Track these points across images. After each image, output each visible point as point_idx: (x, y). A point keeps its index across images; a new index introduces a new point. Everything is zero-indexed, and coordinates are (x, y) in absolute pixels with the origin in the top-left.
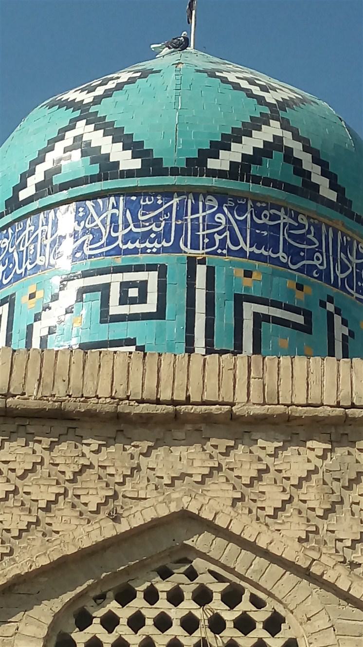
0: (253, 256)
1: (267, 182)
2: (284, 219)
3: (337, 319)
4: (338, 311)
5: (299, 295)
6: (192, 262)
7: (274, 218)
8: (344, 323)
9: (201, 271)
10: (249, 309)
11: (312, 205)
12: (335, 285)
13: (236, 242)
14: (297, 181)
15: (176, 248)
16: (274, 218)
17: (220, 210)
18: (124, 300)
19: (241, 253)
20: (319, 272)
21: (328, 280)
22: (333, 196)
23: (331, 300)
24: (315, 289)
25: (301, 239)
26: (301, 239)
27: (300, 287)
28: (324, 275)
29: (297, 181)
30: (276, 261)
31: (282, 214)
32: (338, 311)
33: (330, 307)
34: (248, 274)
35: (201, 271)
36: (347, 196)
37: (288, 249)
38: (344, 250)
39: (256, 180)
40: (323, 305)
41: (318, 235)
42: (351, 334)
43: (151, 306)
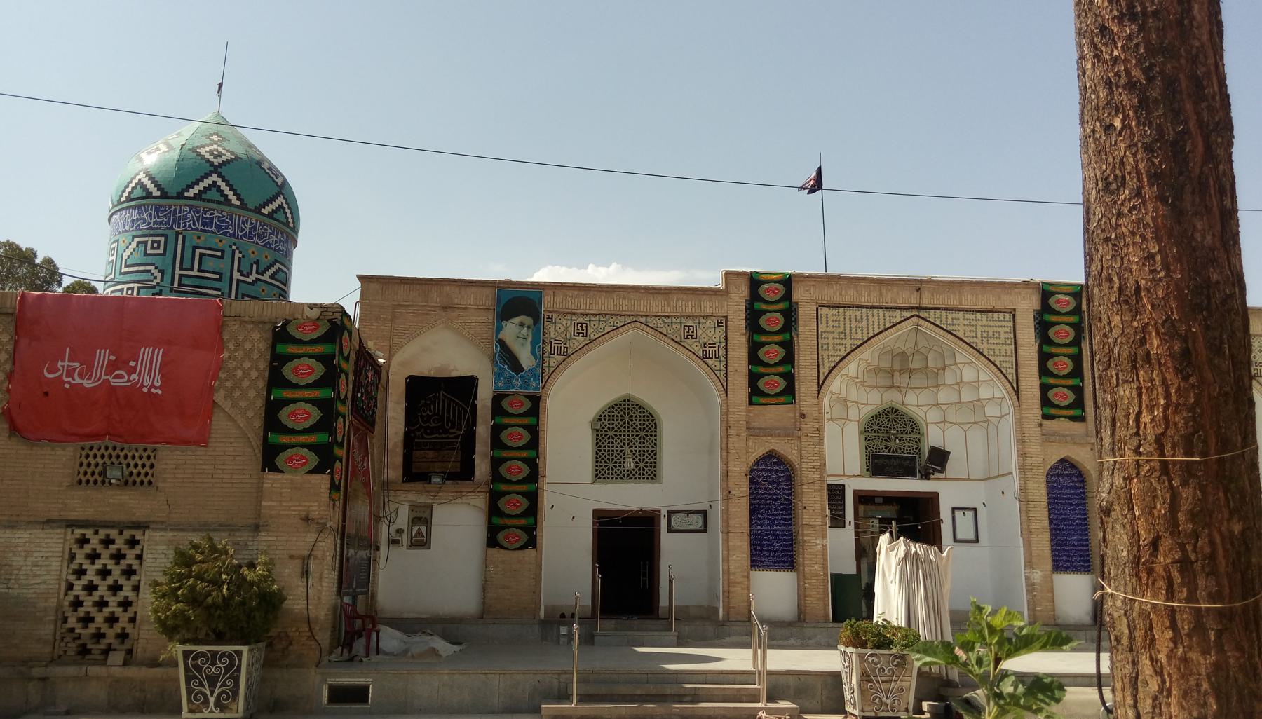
0: (202, 230)
1: (209, 201)
2: (216, 214)
3: (237, 252)
4: (237, 248)
5: (220, 244)
6: (177, 234)
7: (211, 214)
8: (240, 252)
9: (180, 237)
10: (198, 251)
11: (228, 208)
12: (238, 238)
13: (195, 225)
14: (222, 199)
15: (171, 228)
16: (211, 214)
17: (190, 212)
18: (152, 248)
19: (197, 229)
20: (230, 234)
21: (234, 237)
22: (238, 203)
23: (234, 244)
24: (228, 240)
25: (224, 221)
26: (224, 221)
27: (220, 241)
28: (233, 235)
29: (222, 199)
30: (212, 232)
31: (215, 212)
32: (237, 248)
33: (234, 247)
34: (199, 238)
35: (180, 237)
36: (245, 201)
37: (217, 226)
38: (243, 223)
39: (204, 200)
40: (231, 247)
41: (231, 220)
42: (243, 256)
43: (161, 251)
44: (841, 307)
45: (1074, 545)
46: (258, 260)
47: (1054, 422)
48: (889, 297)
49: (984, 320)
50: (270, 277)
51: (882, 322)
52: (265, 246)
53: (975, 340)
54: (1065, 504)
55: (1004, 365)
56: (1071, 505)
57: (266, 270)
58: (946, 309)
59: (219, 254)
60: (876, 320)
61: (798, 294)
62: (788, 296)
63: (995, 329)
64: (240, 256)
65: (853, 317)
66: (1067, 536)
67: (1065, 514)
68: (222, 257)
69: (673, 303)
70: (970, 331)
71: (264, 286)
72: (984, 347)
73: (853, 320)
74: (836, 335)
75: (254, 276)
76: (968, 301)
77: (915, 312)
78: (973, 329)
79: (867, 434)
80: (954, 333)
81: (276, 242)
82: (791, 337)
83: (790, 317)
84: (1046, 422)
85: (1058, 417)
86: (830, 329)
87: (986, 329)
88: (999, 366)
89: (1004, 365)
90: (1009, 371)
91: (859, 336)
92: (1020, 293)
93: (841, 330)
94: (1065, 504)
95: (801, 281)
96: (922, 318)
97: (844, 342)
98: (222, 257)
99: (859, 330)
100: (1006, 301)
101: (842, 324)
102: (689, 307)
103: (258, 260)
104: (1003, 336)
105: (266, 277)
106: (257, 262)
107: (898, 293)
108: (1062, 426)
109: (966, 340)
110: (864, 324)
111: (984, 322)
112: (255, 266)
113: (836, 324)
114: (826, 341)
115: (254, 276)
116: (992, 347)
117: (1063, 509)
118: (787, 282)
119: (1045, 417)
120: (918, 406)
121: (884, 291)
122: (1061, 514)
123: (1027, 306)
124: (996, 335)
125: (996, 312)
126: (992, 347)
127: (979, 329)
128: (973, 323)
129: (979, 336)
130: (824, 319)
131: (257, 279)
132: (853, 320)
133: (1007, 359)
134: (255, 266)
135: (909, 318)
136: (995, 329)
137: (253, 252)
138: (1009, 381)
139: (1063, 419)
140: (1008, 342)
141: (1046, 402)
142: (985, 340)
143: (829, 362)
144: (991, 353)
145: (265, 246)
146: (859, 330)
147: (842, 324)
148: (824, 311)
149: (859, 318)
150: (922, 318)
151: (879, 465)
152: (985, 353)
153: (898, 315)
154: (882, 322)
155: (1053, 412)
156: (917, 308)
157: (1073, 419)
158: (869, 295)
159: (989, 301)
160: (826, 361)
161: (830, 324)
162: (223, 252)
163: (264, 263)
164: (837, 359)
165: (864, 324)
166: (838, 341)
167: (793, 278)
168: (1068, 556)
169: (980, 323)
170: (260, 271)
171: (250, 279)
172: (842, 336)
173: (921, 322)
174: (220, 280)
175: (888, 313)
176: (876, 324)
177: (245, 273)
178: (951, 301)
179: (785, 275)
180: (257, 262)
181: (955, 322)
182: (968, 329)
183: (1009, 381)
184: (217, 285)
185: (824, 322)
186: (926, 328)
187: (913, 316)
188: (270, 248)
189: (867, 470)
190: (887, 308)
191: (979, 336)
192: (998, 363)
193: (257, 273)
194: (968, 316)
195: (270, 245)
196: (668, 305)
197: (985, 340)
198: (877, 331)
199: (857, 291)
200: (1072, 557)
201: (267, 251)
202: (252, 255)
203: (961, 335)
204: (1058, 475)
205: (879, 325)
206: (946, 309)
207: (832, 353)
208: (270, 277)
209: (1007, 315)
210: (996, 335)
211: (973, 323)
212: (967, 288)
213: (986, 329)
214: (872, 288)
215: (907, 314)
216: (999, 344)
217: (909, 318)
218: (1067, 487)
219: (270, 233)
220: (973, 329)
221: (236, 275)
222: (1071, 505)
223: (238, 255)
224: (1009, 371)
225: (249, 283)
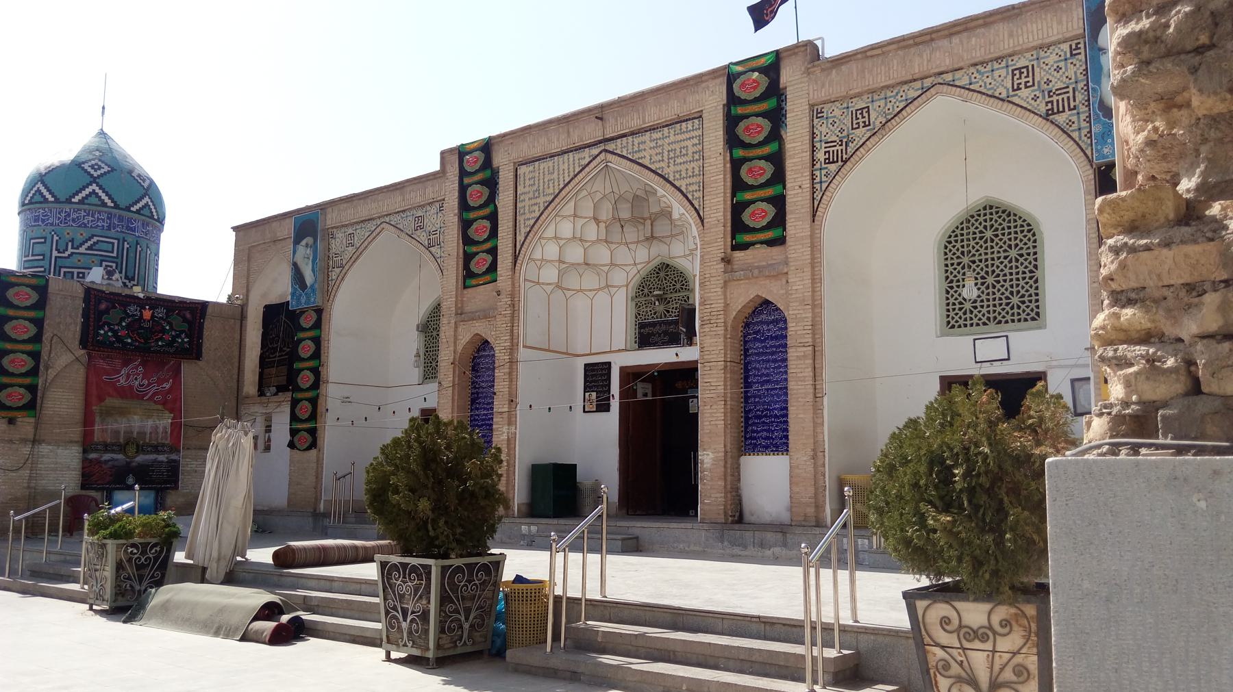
42: (60, 238)
44: (537, 161)
45: (776, 416)
46: (73, 239)
47: (748, 252)
48: (576, 138)
49: (670, 135)
50: (86, 249)
51: (571, 169)
52: (79, 226)
53: (662, 164)
54: (768, 361)
55: (690, 189)
56: (775, 361)
57: (81, 245)
58: (633, 134)
59: (43, 240)
60: (567, 165)
61: (501, 160)
62: (487, 163)
63: (683, 144)
64: (58, 238)
65: (546, 170)
66: (769, 404)
67: (767, 375)
68: (45, 242)
69: (407, 196)
70: (656, 155)
71: (79, 257)
72: (669, 172)
73: (546, 173)
74: (531, 195)
75: (70, 250)
76: (653, 115)
77: (602, 147)
78: (660, 150)
79: (637, 300)
80: (640, 161)
81: (92, 221)
82: (496, 207)
83: (492, 184)
84: (738, 255)
85: (753, 244)
86: (527, 189)
87: (673, 146)
88: (685, 191)
89: (690, 189)
90: (696, 195)
91: (551, 191)
92: (708, 87)
93: (535, 188)
94: (768, 361)
95: (501, 141)
96: (610, 152)
97: (538, 200)
98: (45, 242)
99: (551, 185)
100: (691, 104)
101: (536, 182)
102: (415, 197)
103: (73, 239)
104: (690, 152)
105: (82, 250)
106: (72, 241)
107: (584, 129)
108: (758, 255)
109: (653, 167)
110: (555, 175)
111: (672, 139)
112: (70, 244)
113: (532, 182)
114: (522, 204)
115: (70, 250)
116: (678, 168)
117: (766, 368)
118: (487, 147)
119: (734, 248)
120: (685, 256)
121: (571, 130)
122: (763, 375)
123: (713, 102)
124: (684, 152)
125: (684, 121)
126: (678, 168)
127: (667, 148)
128: (660, 142)
129: (666, 158)
130: (522, 179)
131: (72, 253)
132: (546, 173)
133: (694, 180)
134: (70, 244)
135: (598, 155)
136: (683, 144)
137: (68, 234)
138: (695, 209)
139: (758, 246)
140: (697, 157)
141: (738, 226)
142: (672, 161)
143: (524, 227)
144: (678, 176)
145: (79, 226)
146: (551, 185)
147: (536, 182)
148: (523, 170)
149: (551, 169)
150: (610, 152)
151: (646, 337)
152: (671, 179)
153: (586, 155)
154: (571, 169)
155: (747, 238)
156: (600, 142)
157: (771, 243)
158: (558, 140)
159: (674, 109)
160: (522, 226)
161: (527, 183)
162: (45, 238)
163: (79, 239)
164: (532, 222)
165: (555, 175)
166: (533, 201)
167: (492, 142)
168: (768, 431)
169: (667, 141)
170: (75, 246)
171: (66, 254)
172: (537, 194)
173: (610, 157)
174: (43, 260)
175: (577, 155)
176: (566, 172)
177: (61, 250)
178: (634, 122)
179: (485, 139)
180: (72, 241)
181: (642, 147)
182: (653, 152)
183: (695, 209)
184: (41, 263)
185: (522, 183)
186: (616, 163)
187: (601, 152)
188: (86, 226)
189: (636, 342)
190: (576, 150)
191: (666, 158)
192: (683, 189)
193: (72, 248)
194: (656, 135)
195: (85, 224)
196: (404, 200)
197: (672, 161)
198: (567, 180)
199: (548, 139)
200: (773, 431)
201: (82, 230)
202: (68, 236)
203: (646, 162)
204: (762, 322)
205: (569, 172)
206: (633, 134)
207: (527, 216)
208: (86, 249)
209: (696, 121)
210: (684, 152)
211: (660, 142)
212: (651, 100)
213: (673, 146)
214: (561, 130)
215: (595, 151)
216: (687, 162)
217: (598, 155)
218: (772, 338)
219: (84, 216)
220: (660, 150)
221: (55, 253)
222: (775, 361)
223: (56, 238)
224: (696, 195)
225: (65, 257)
